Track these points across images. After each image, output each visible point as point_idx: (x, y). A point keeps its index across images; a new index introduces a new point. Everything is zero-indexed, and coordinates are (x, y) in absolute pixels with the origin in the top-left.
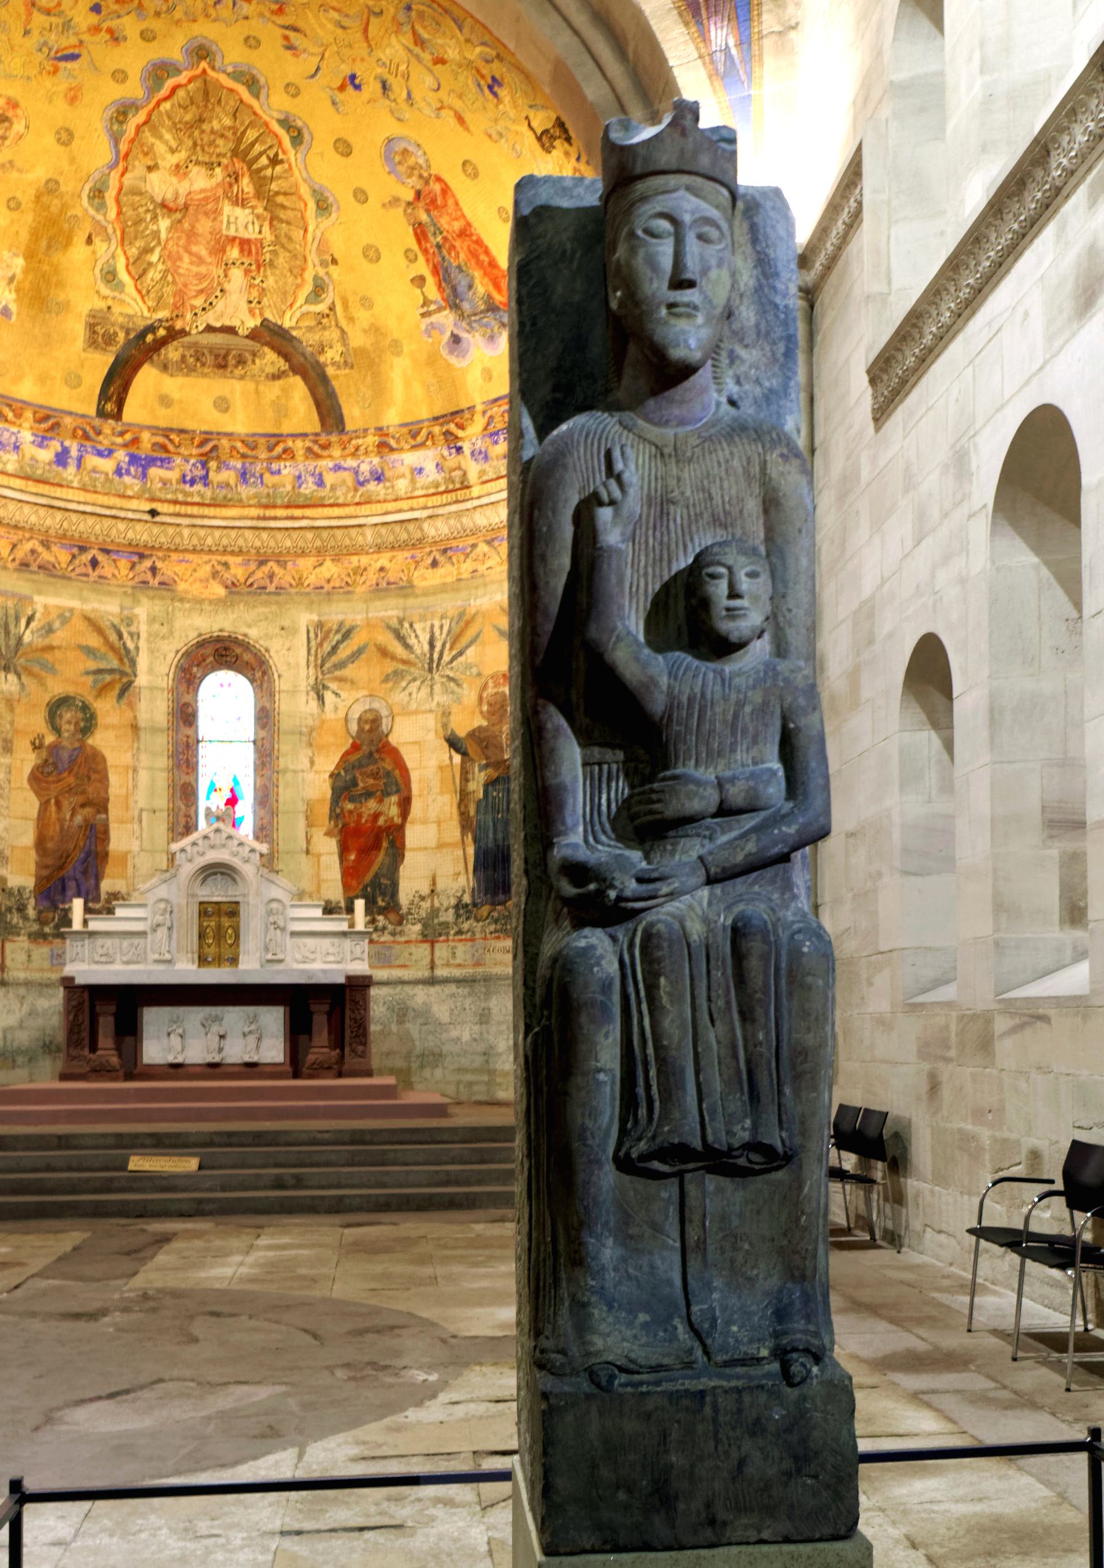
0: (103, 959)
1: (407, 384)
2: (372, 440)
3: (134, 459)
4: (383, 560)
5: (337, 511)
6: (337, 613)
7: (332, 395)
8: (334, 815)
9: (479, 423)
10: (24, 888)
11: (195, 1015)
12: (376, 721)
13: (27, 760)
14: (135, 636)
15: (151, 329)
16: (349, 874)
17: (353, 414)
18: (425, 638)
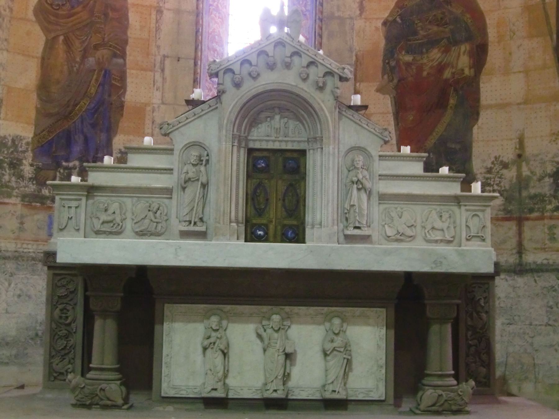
0: (106, 228)
10: (21, 139)
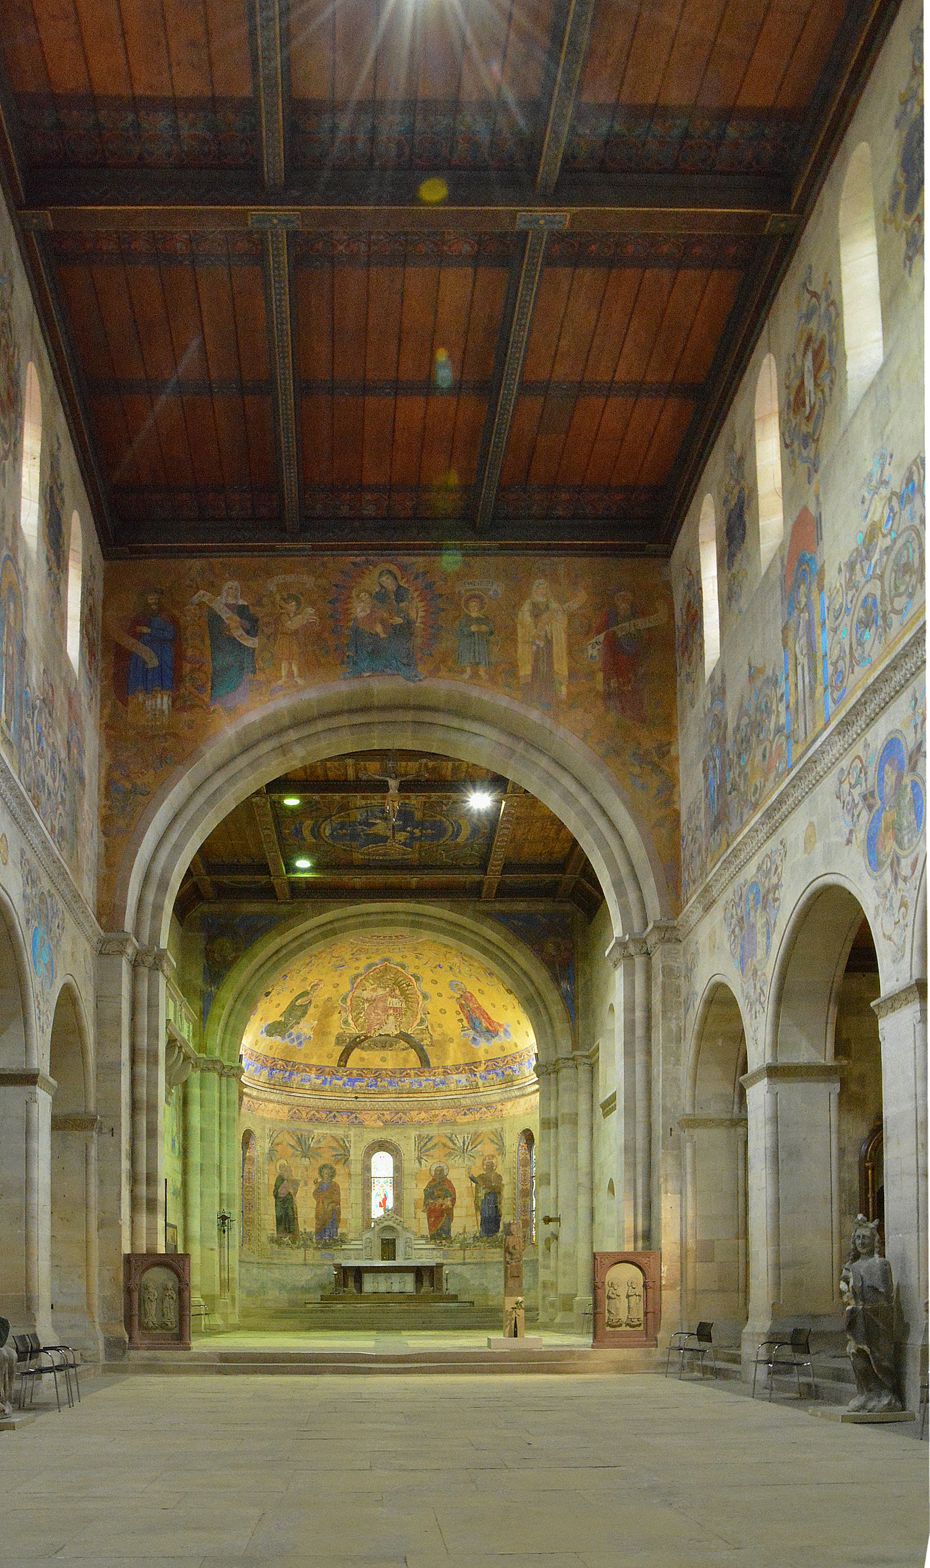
1: (455, 1052)
2: (441, 1070)
3: (350, 1080)
4: (445, 1112)
5: (426, 1095)
6: (425, 1131)
7: (426, 1056)
8: (426, 1205)
9: (483, 1067)
11: (381, 1277)
12: (442, 1171)
13: (312, 1188)
14: (349, 1142)
15: (359, 1037)
16: (431, 1225)
17: (433, 1062)
18: (461, 1141)
